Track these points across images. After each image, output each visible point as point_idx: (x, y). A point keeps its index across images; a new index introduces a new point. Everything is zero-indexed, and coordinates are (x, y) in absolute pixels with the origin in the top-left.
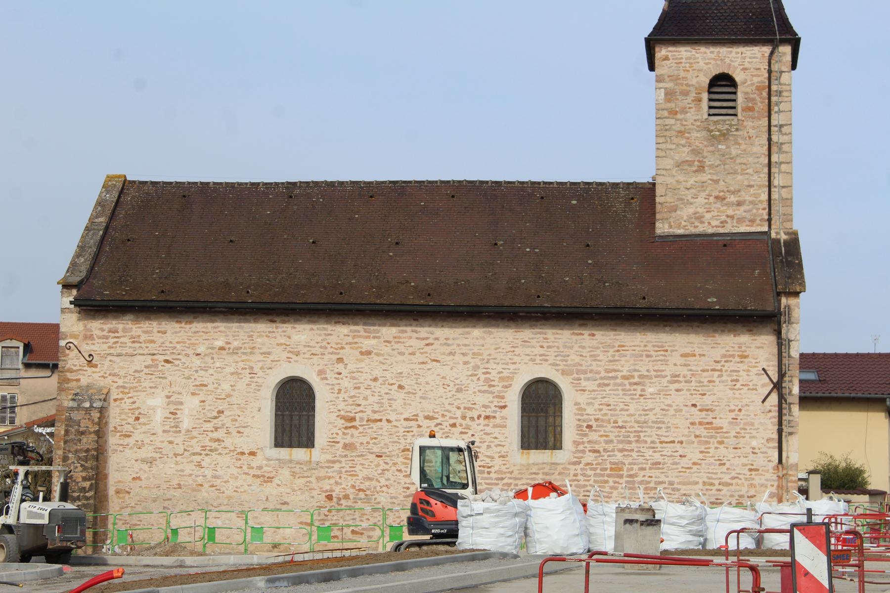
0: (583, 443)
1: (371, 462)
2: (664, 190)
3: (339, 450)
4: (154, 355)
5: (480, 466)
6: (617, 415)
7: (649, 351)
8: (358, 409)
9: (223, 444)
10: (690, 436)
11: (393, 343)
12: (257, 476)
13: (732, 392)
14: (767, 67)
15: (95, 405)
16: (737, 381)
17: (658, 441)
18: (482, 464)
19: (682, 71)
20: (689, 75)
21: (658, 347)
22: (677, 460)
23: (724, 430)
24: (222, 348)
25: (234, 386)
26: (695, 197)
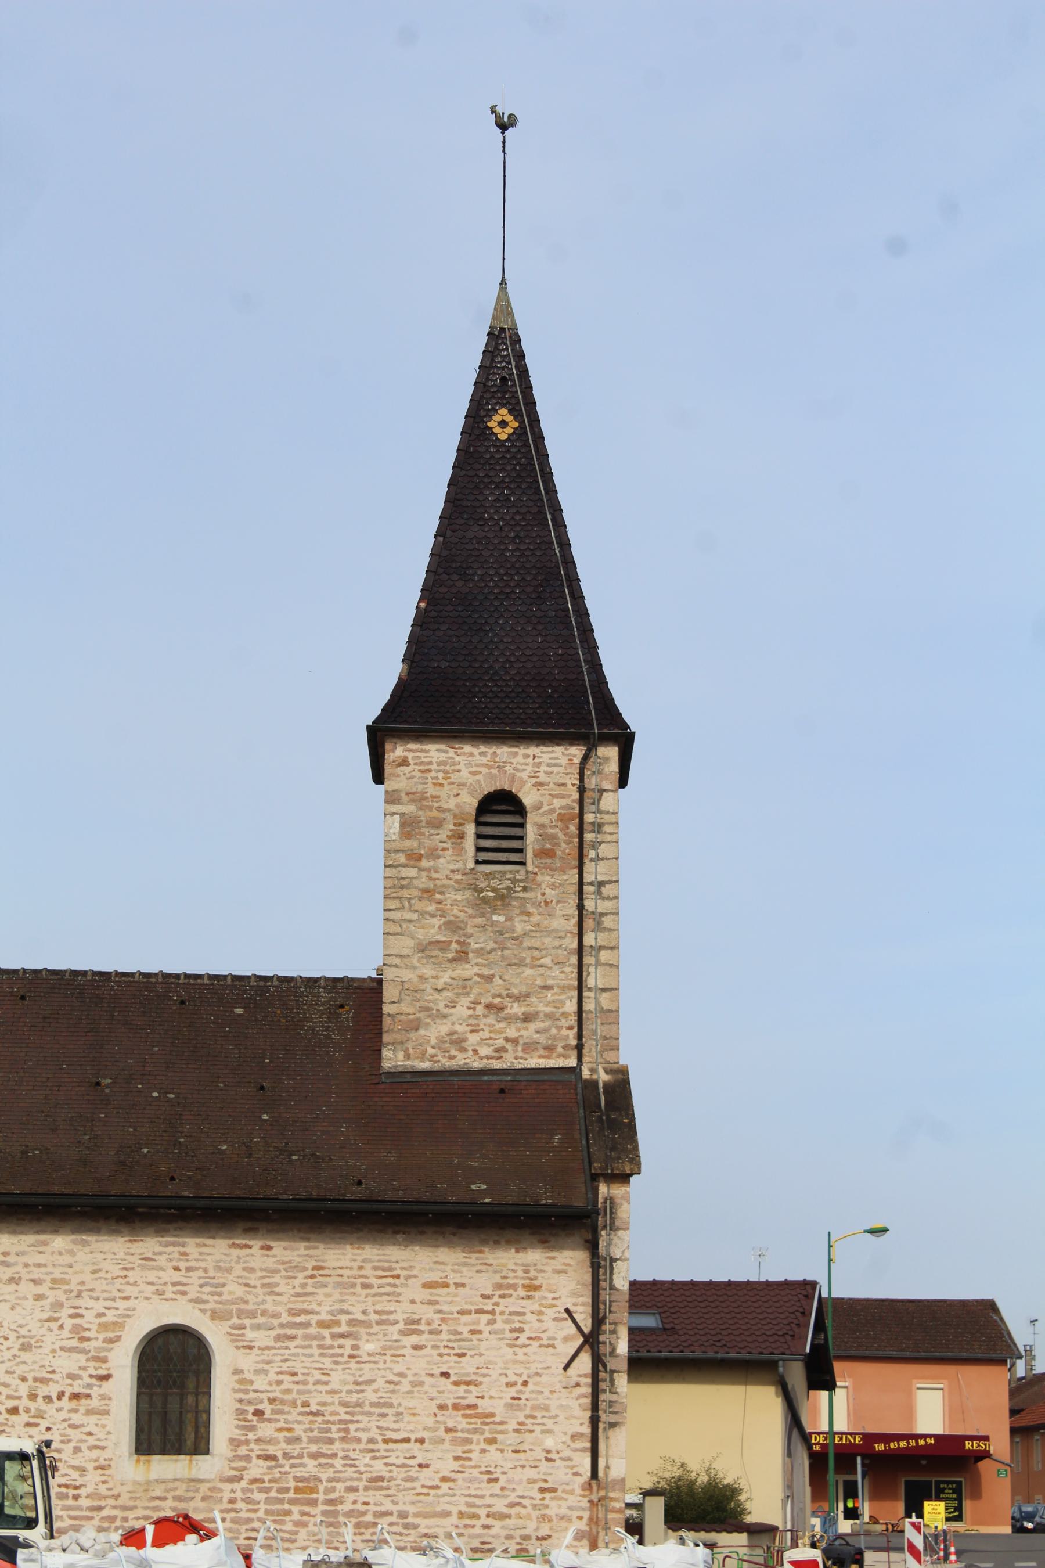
2: (397, 992)
5: (60, 1486)
6: (309, 1392)
10: (436, 1429)
13: (511, 1351)
14: (577, 782)
16: (521, 1330)
17: (380, 1438)
18: (63, 1481)
19: (430, 785)
20: (443, 793)
21: (384, 1269)
22: (414, 1472)
23: (497, 1419)
26: (452, 1004)
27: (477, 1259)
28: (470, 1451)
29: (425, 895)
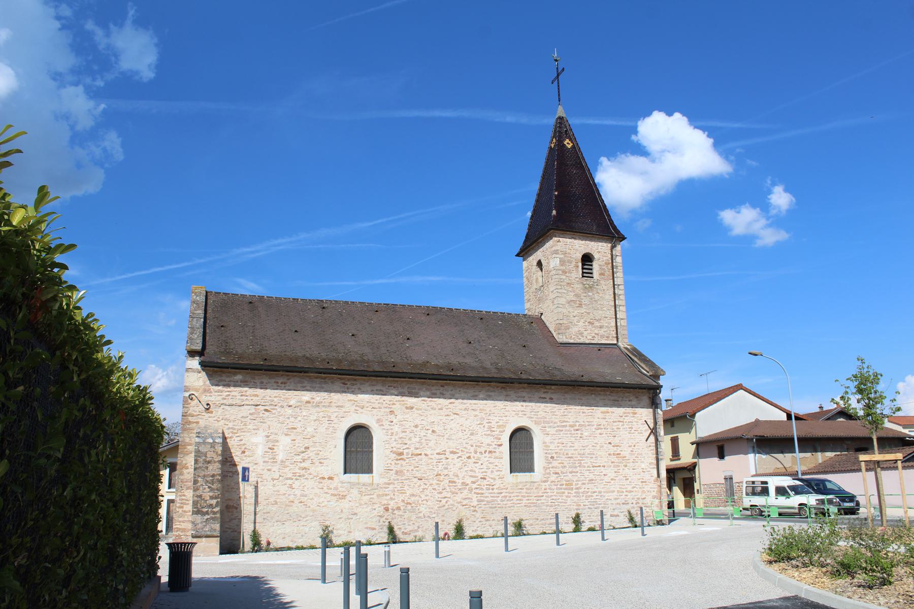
0: (549, 468)
3: (393, 476)
4: (257, 405)
5: (487, 485)
7: (584, 410)
8: (405, 446)
11: (428, 402)
12: (332, 495)
15: (217, 441)
16: (632, 428)
20: (571, 252)
23: (627, 458)
24: (308, 402)
25: (317, 429)
28: (619, 469)
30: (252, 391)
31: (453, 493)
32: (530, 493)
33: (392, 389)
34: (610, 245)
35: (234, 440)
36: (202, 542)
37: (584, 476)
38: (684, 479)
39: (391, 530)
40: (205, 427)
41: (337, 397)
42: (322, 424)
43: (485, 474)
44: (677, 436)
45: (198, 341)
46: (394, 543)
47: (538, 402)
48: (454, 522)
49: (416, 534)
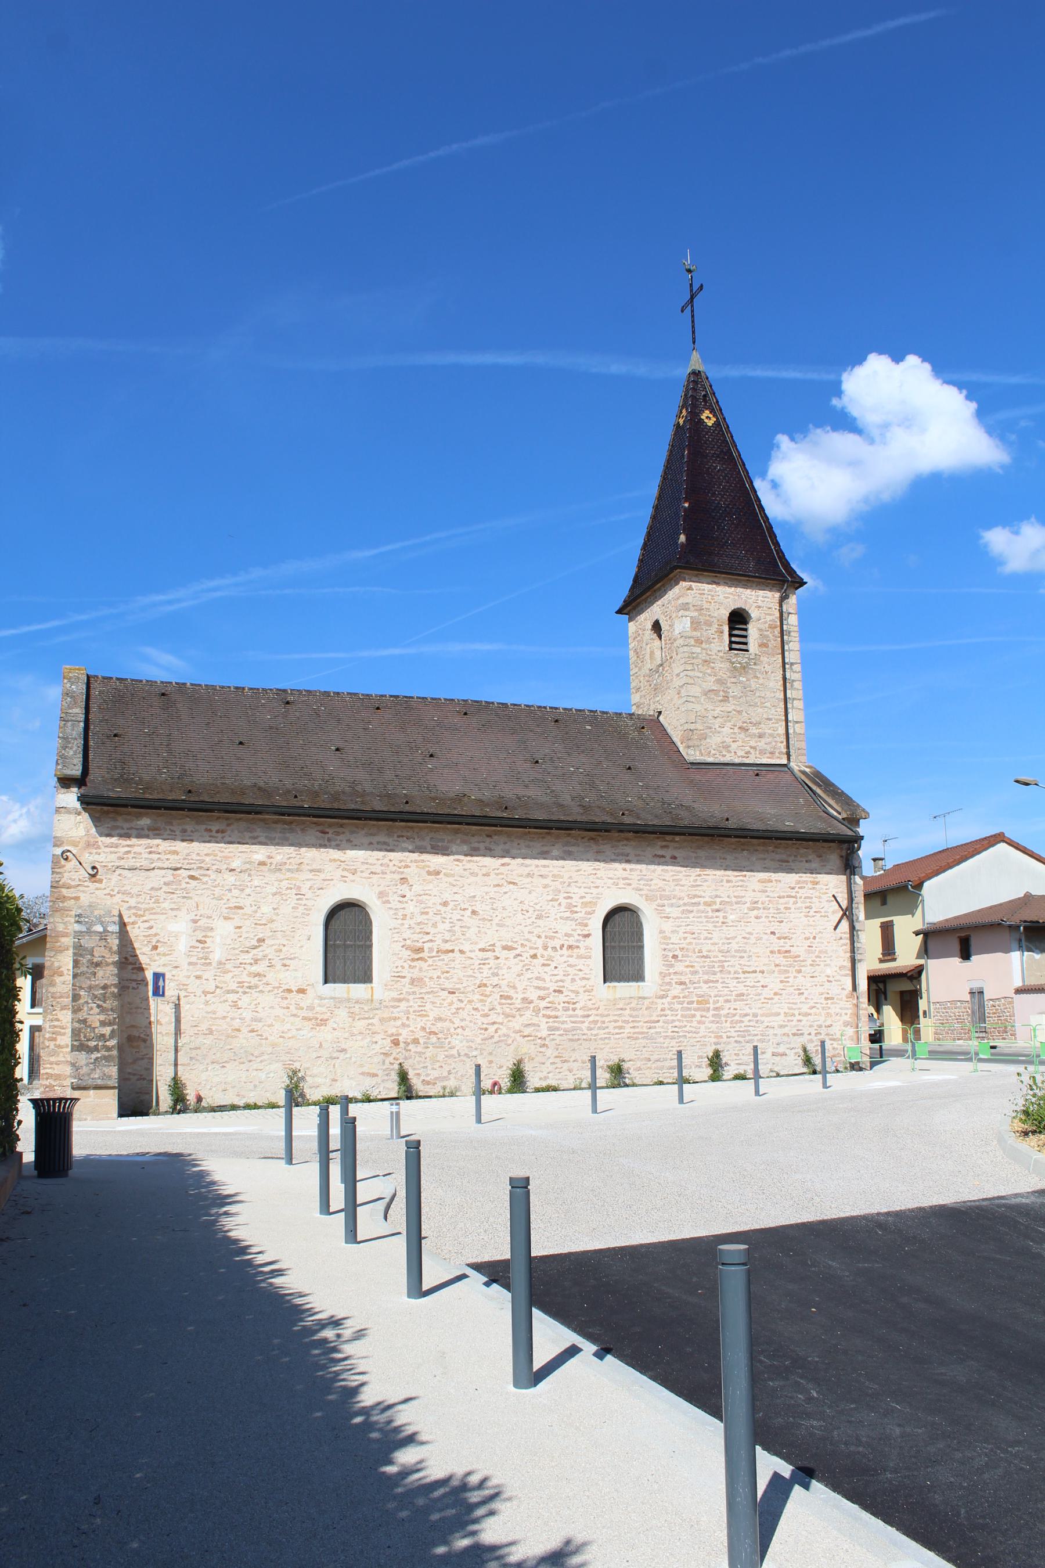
0: (670, 974)
1: (444, 1000)
5: (564, 1003)
7: (729, 876)
8: (427, 938)
9: (265, 980)
12: (304, 1018)
14: (778, 608)
15: (110, 929)
16: (810, 908)
17: (741, 971)
23: (801, 959)
24: (262, 864)
27: (786, 866)
28: (788, 977)
29: (705, 664)
30: (169, 845)
31: (507, 1016)
32: (637, 1016)
33: (404, 842)
34: (777, 595)
35: (139, 928)
36: (89, 1097)
37: (728, 987)
38: (902, 993)
39: (403, 1077)
40: (90, 906)
41: (312, 856)
42: (286, 900)
43: (561, 984)
44: (892, 921)
45: (75, 761)
46: (409, 1098)
47: (652, 863)
48: (509, 1064)
49: (445, 1083)
